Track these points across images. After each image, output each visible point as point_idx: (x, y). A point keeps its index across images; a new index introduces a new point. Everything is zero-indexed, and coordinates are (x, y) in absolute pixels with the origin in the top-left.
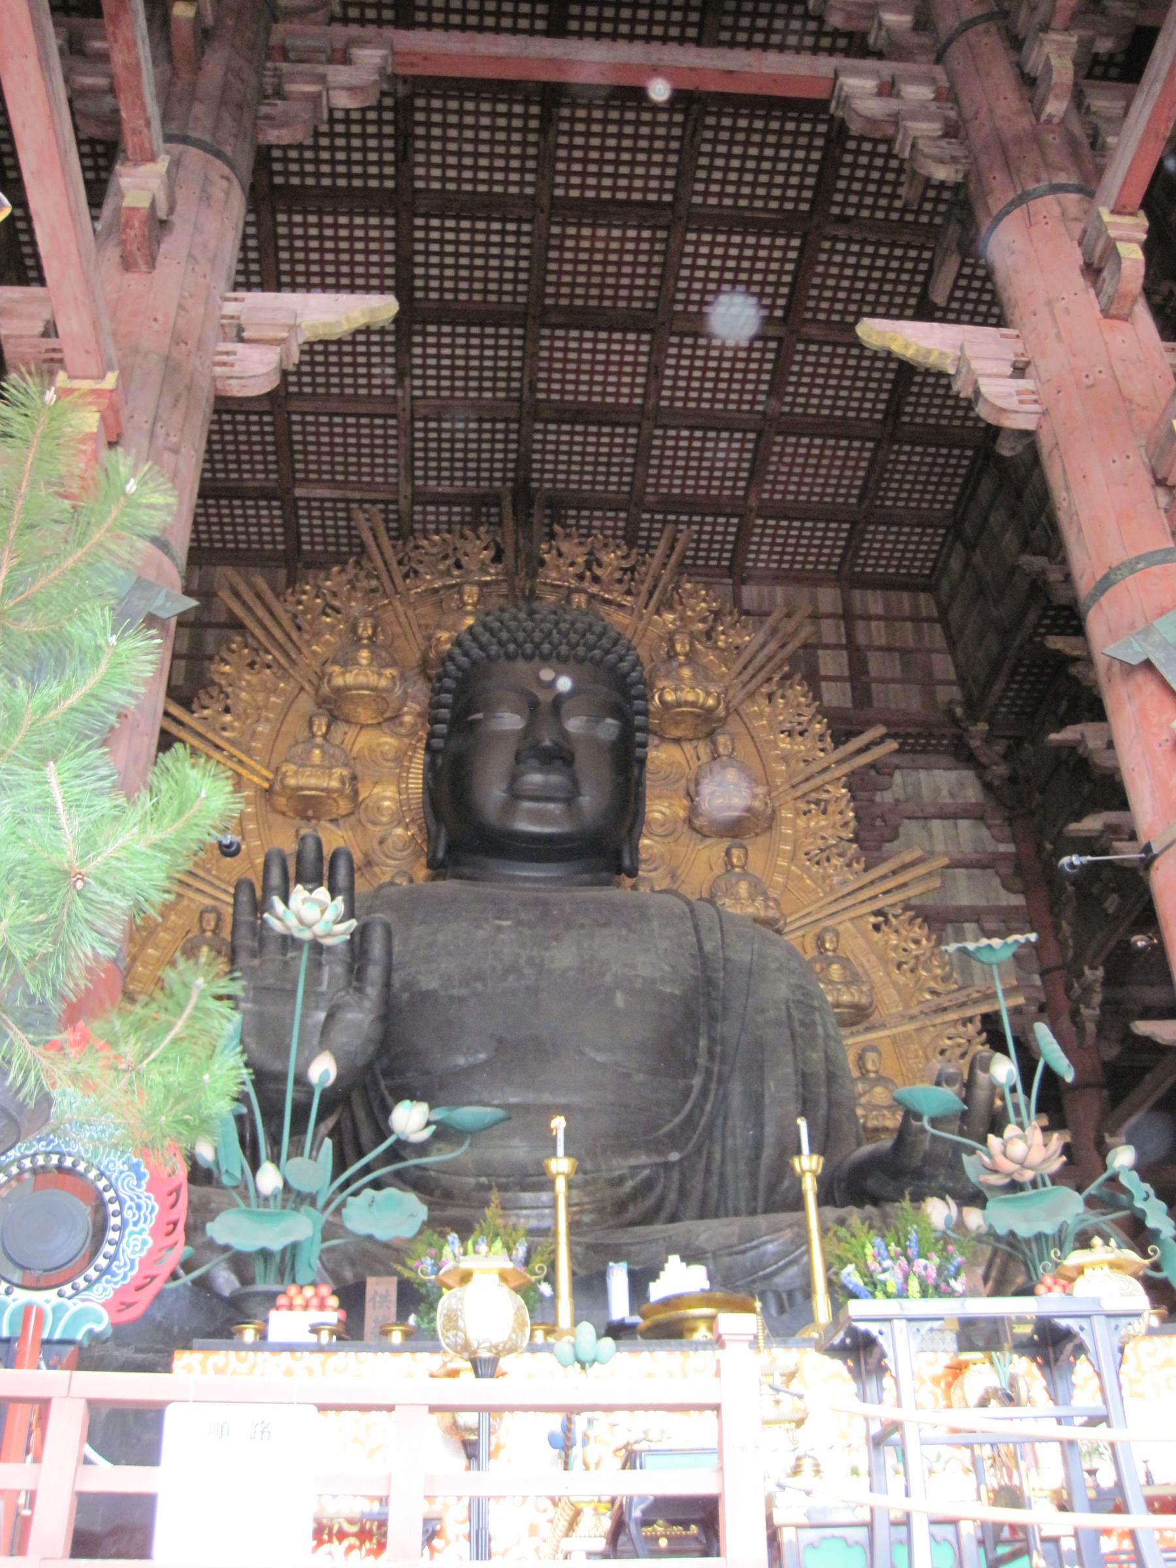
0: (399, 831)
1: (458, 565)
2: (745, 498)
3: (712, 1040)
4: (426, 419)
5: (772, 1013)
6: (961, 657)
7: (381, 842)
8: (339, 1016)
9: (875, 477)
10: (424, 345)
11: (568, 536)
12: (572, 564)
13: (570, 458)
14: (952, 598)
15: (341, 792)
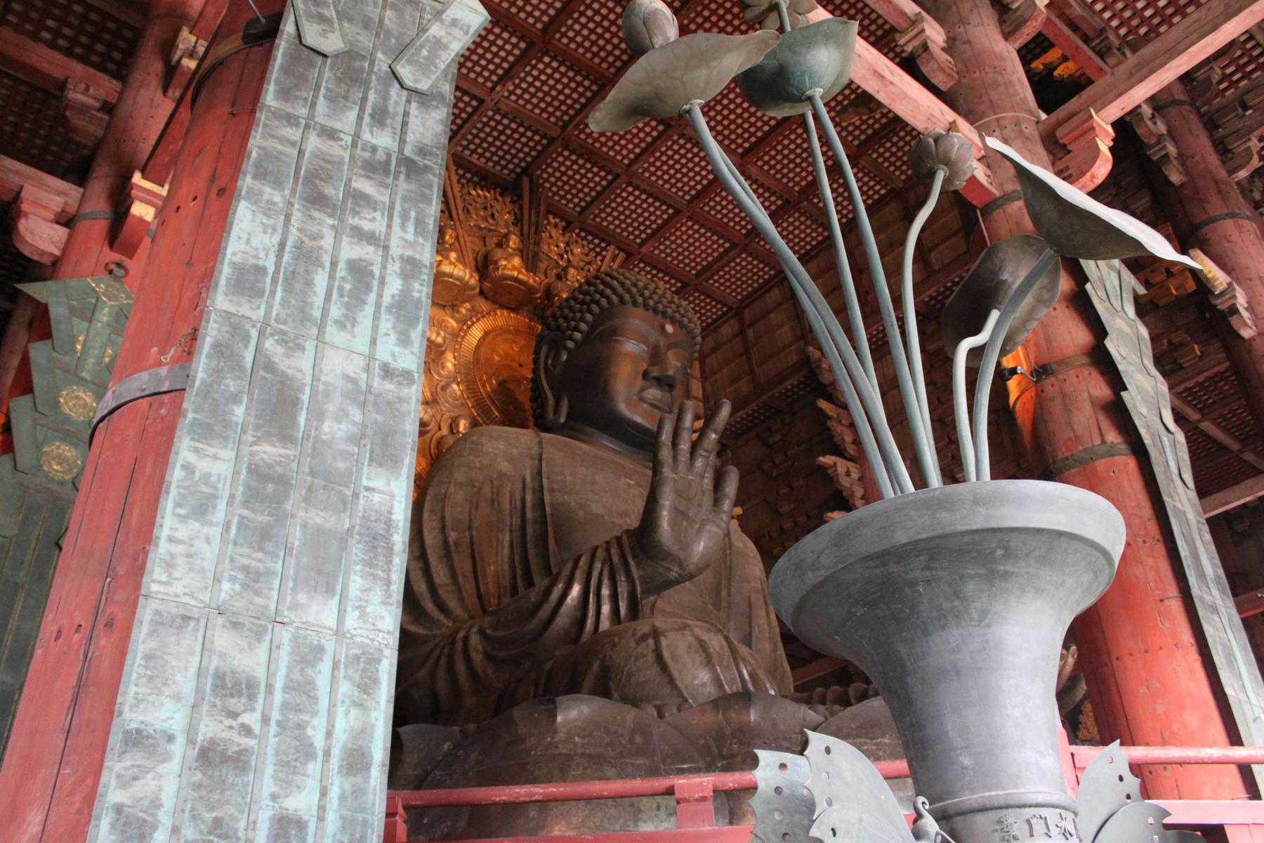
0: (455, 387)
1: (493, 216)
2: (641, 245)
3: (729, 594)
4: (497, 112)
5: (753, 584)
6: (708, 386)
7: (443, 389)
8: (708, 527)
9: (719, 264)
10: (534, 67)
11: (556, 226)
12: (557, 246)
13: (568, 178)
14: (714, 350)
15: (440, 346)
